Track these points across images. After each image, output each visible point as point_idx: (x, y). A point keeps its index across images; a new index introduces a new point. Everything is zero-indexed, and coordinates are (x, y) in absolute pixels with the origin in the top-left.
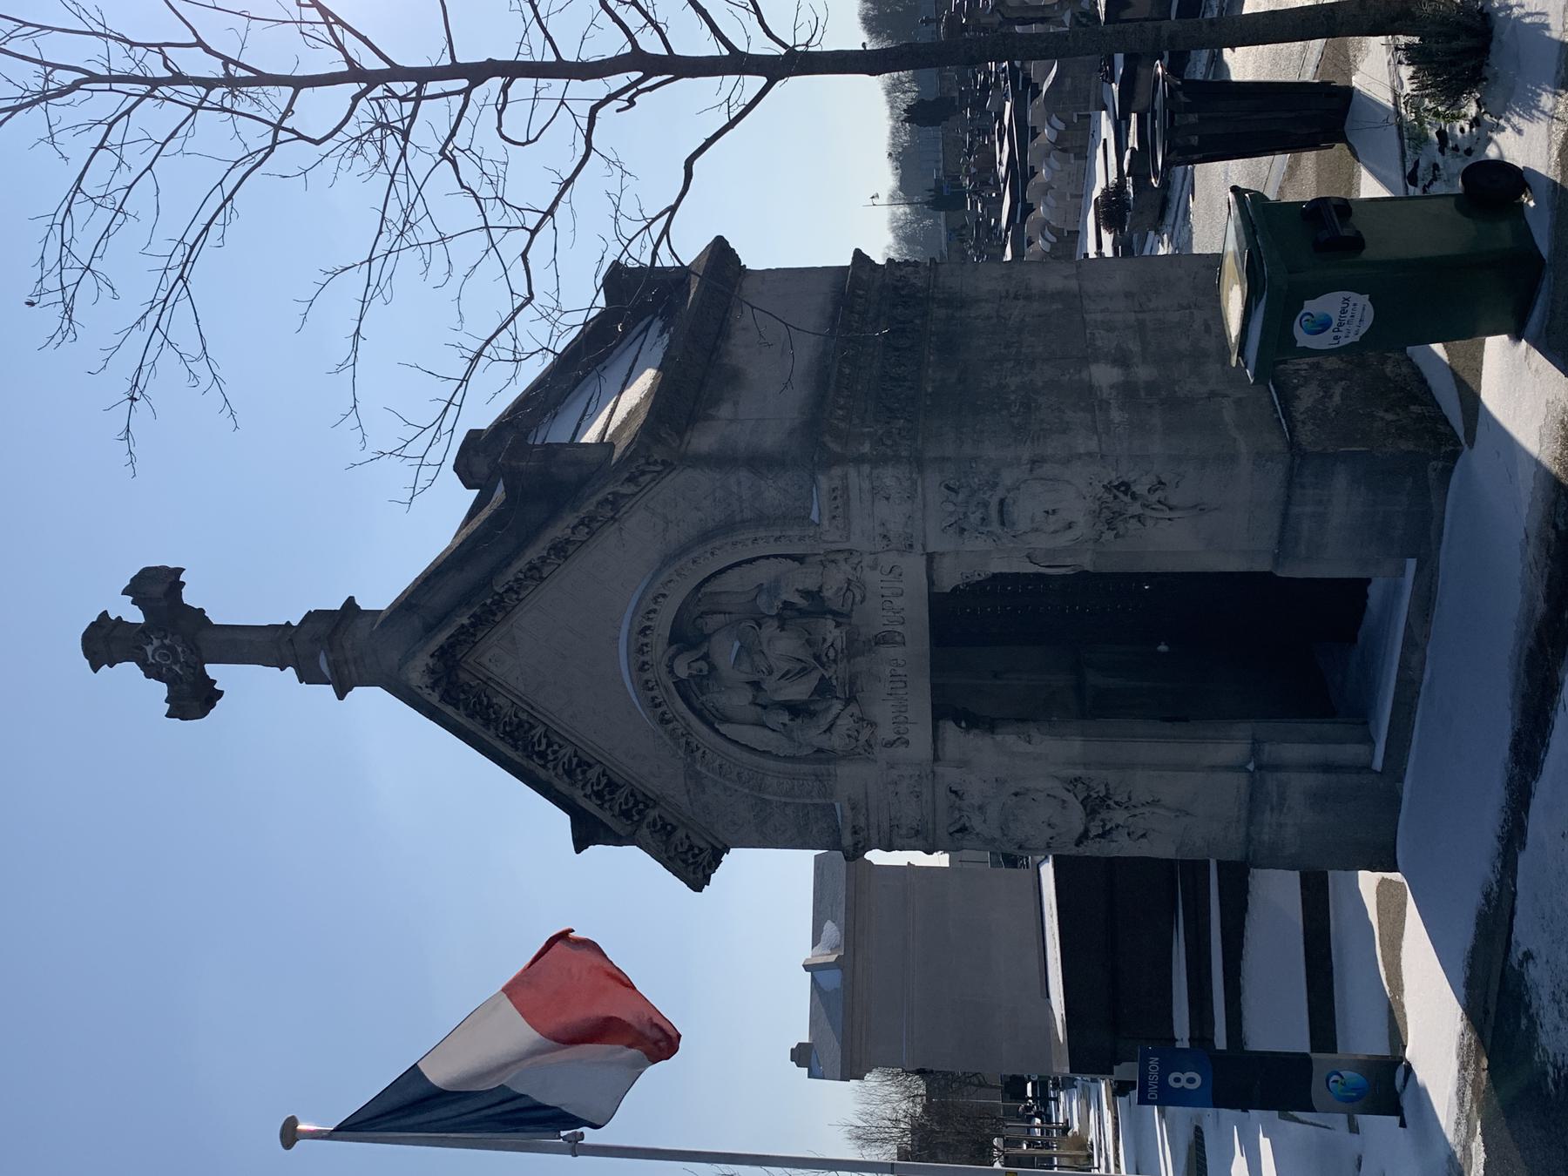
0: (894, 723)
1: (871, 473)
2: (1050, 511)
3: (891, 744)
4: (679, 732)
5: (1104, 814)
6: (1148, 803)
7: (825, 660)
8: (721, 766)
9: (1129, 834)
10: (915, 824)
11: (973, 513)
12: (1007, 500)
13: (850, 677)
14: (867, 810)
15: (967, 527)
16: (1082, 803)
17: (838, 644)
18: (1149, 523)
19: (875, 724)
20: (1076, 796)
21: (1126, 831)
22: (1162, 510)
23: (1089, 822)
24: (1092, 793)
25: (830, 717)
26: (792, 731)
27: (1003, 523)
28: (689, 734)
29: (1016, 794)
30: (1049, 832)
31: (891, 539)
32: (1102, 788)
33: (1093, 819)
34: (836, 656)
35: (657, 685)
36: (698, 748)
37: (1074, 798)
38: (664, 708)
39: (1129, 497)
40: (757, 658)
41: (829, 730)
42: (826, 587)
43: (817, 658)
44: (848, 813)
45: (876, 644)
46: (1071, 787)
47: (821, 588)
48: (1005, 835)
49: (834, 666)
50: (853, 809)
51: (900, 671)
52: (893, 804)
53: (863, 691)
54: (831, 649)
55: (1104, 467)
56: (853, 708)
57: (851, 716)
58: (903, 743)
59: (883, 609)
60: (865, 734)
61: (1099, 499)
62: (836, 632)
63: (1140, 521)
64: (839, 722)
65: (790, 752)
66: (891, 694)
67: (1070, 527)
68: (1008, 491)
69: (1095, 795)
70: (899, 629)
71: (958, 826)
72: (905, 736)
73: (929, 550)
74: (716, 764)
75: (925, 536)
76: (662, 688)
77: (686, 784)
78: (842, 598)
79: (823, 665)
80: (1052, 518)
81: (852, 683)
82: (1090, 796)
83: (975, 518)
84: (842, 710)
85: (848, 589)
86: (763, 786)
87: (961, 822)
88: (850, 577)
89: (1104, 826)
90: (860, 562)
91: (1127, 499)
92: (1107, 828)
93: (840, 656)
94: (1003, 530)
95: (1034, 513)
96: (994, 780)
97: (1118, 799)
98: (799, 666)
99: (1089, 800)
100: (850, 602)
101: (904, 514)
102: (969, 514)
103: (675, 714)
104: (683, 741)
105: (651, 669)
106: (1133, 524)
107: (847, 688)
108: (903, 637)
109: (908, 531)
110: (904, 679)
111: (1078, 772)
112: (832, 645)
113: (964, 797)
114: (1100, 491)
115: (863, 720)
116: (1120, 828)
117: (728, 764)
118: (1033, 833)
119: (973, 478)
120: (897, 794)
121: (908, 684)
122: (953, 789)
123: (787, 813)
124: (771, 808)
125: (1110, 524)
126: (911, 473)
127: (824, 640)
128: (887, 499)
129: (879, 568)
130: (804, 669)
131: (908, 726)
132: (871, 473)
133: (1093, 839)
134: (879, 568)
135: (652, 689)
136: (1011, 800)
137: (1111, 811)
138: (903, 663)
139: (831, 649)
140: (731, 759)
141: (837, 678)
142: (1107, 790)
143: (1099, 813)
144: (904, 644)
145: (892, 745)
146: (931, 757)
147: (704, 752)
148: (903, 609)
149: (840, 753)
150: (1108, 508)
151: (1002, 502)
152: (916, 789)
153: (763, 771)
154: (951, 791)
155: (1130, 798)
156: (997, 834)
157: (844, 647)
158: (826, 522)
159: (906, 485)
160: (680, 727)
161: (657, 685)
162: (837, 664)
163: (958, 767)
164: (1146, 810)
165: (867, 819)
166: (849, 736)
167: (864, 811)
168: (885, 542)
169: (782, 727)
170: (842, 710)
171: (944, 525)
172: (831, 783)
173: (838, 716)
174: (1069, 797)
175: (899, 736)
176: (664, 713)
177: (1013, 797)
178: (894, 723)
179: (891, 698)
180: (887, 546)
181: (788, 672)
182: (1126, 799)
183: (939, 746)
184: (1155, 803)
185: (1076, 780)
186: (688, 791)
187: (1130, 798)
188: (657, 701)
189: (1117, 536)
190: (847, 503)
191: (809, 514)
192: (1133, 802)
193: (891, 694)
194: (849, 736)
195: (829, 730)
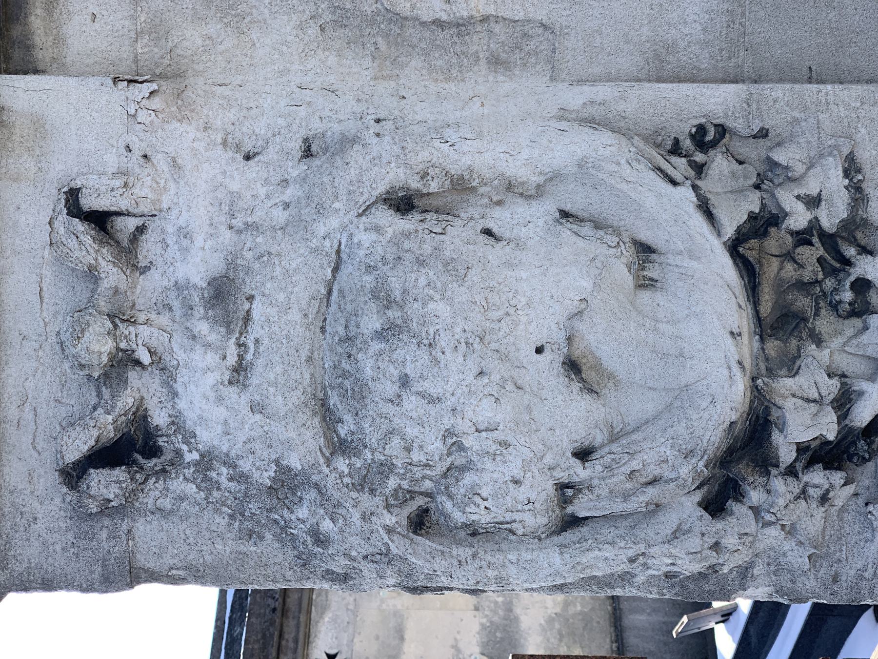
16: (734, 248)
20: (706, 209)
23: (771, 373)
24: (787, 199)
37: (698, 221)
87: (126, 401)
96: (296, 146)
113: (149, 247)
118: (486, 412)
122: (89, 202)
133: (791, 472)
136: (378, 229)
143: (819, 342)
177: (385, 217)
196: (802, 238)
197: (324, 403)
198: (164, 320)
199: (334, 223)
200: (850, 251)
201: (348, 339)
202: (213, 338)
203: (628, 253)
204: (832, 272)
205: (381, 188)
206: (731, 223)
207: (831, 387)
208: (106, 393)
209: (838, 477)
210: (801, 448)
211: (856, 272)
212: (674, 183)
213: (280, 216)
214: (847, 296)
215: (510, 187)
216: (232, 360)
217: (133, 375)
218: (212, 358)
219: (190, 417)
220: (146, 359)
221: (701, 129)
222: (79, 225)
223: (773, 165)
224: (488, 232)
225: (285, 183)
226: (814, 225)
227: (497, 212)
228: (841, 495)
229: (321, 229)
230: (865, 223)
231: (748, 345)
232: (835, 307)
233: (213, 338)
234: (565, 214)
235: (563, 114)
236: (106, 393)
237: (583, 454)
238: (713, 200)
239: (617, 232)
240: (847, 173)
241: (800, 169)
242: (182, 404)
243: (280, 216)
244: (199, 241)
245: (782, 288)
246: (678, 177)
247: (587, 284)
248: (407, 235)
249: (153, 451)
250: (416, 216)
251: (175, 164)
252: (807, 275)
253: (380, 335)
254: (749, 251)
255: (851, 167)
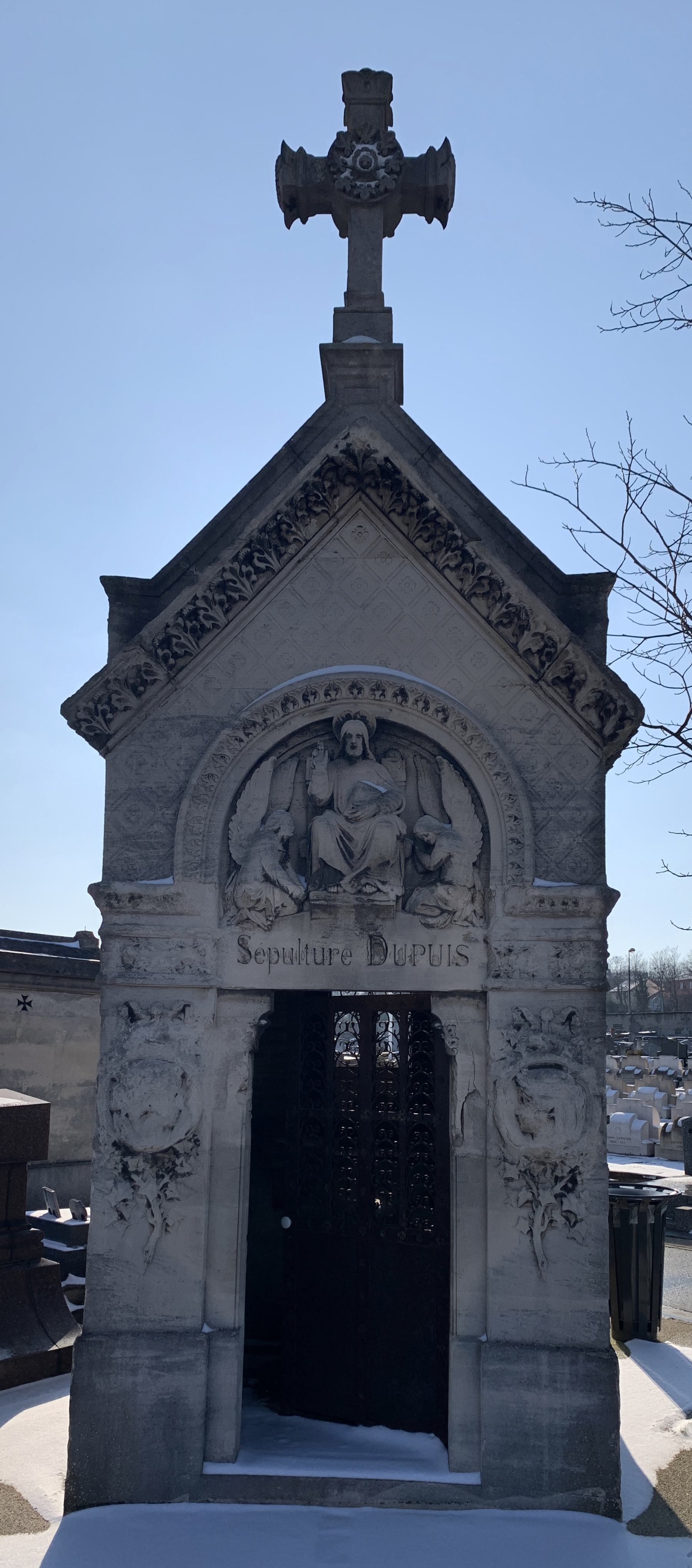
0: (269, 949)
1: (589, 940)
2: (552, 1115)
3: (242, 943)
4: (270, 716)
5: (150, 1172)
6: (165, 1219)
7: (363, 881)
8: (223, 757)
9: (124, 1201)
10: (141, 964)
11: (543, 1039)
12: (563, 1073)
13: (334, 906)
14: (160, 914)
15: (521, 1031)
16: (171, 1147)
17: (378, 897)
18: (525, 1212)
19: (269, 930)
21: (130, 1197)
22: (543, 1225)
24: (182, 1159)
25: (285, 883)
26: (271, 839)
27: (531, 1068)
28: (266, 727)
29: (184, 1076)
30: (136, 1113)
31: (507, 957)
32: (186, 1169)
33: (146, 1161)
34: (366, 894)
35: (330, 701)
36: (247, 735)
37: (178, 1139)
38: (301, 704)
39: (560, 1191)
40: (372, 808)
41: (267, 878)
42: (451, 890)
43: (366, 872)
44: (160, 892)
45: (371, 937)
46: (190, 1136)
47: (450, 883)
48: (131, 1063)
49: (353, 891)
50: (165, 898)
51: (337, 959)
52: (167, 943)
53: (312, 919)
54: (375, 890)
55: (594, 1166)
56: (291, 907)
57: (282, 905)
58: (244, 957)
59: (414, 946)
60: (258, 918)
61: (562, 1162)
62: (392, 896)
63: (527, 1202)
64: (277, 891)
65: (234, 835)
66: (307, 948)
67: (524, 1133)
68: (574, 1074)
69: (178, 1162)
70: (390, 960)
71: (137, 1011)
72: (253, 960)
73: (491, 995)
74: (226, 752)
75: (510, 990)
76: (324, 705)
77: (195, 716)
78: (434, 904)
79: (358, 877)
80: (544, 1116)
81: (324, 908)
82: (178, 1157)
83: (537, 1040)
84: (291, 896)
85: (443, 911)
86: (198, 801)
87: (143, 1016)
88: (457, 914)
89: (137, 1173)
90: (474, 926)
91: (558, 1189)
92: (134, 1177)
93: (365, 898)
94: (524, 1067)
95: (552, 1098)
96: (198, 1053)
97: (172, 1186)
98: (357, 851)
99: (172, 1156)
100: (428, 912)
101: (536, 971)
102: (541, 1034)
103: (291, 715)
104: (259, 720)
105: (351, 696)
106: (525, 1195)
107: (322, 902)
108: (379, 964)
109: (516, 974)
110: (327, 962)
111: (206, 1144)
112: (379, 890)
113: (177, 1021)
114: (571, 1163)
115: (276, 917)
116: (132, 1191)
117: (225, 765)
119: (583, 1040)
120: (182, 947)
121: (320, 966)
122: (187, 1009)
123: (155, 826)
124: (161, 808)
125: (526, 1173)
126: (589, 979)
127: (384, 883)
128: (558, 956)
129: (467, 944)
130: (351, 855)
131: (266, 963)
132: (589, 940)
133: (122, 1161)
134: (467, 944)
135: (327, 694)
136: (177, 1071)
137: (155, 1180)
138: (347, 962)
139: (375, 890)
140: (230, 768)
141: (337, 892)
142: (183, 1175)
143: (151, 1168)
144: (371, 964)
145: (240, 945)
146: (224, 987)
147: (241, 741)
148: (414, 965)
149: (231, 889)
150: (545, 1171)
151: (558, 1067)
152: (187, 968)
153: (213, 802)
154: (185, 1006)
155: (171, 1199)
156: (131, 1055)
157: (375, 903)
158: (537, 893)
159: (574, 974)
160: (276, 717)
161: (330, 701)
162: (354, 894)
163: (214, 1015)
164: (158, 1218)
165: (147, 913)
166: (259, 901)
167: (159, 910)
168: (503, 951)
169: (276, 828)
170: (291, 896)
171: (524, 1010)
172: (198, 877)
173: (284, 890)
174: (180, 1133)
175: (253, 953)
176: (294, 703)
178: (269, 949)
179: (303, 948)
180: (499, 953)
181: (350, 839)
182: (169, 1195)
183: (237, 996)
184: (166, 1226)
185: (197, 1141)
186: (184, 718)
187: (171, 1199)
188: (311, 698)
189: (510, 1180)
190: (554, 916)
191: (540, 877)
192: (165, 1203)
193: (307, 948)
194: (259, 901)
195: (267, 878)
196: (174, 1164)
197: (141, 1060)
198: (161, 1024)
199: (180, 1062)
200: (171, 1174)
201: (154, 1065)
202: (156, 1036)
203: (171, 1125)
204: (166, 1170)
205: (187, 1072)
206: (177, 1147)
207: (140, 1170)
208: (145, 1011)
209: (120, 1171)
210: (127, 1163)
211: (166, 1175)
212: (186, 1134)
213: (182, 1050)
214: (161, 1173)
215: (187, 1099)
216: (151, 1040)
217: (149, 1017)
218: (151, 1035)
219: (139, 1030)
220: (152, 1021)
221: (199, 1141)
222: (182, 1007)
223: (190, 1157)
224: (177, 1094)
225: (190, 1051)
226: (176, 1165)
227: (182, 1096)
228: (116, 1173)
229: (179, 1059)
230: (177, 1177)
231: (150, 1151)
232: (159, 1171)
233: (156, 1036)
234: (180, 1111)
235: (203, 1111)
236: (145, 1011)
237: (127, 1115)
238: (182, 1143)
239: (177, 1122)
240: (188, 1173)
241: (189, 1162)
242: (142, 1028)
243: (182, 1050)
244: (178, 1033)
245: (164, 1158)
246: (188, 1135)
247: (164, 1116)
248: (176, 1077)
249: (132, 1021)
250: (181, 1079)
251: (195, 1027)
252: (166, 1164)
253: (154, 1072)
254: (171, 1151)
255: (189, 1174)
